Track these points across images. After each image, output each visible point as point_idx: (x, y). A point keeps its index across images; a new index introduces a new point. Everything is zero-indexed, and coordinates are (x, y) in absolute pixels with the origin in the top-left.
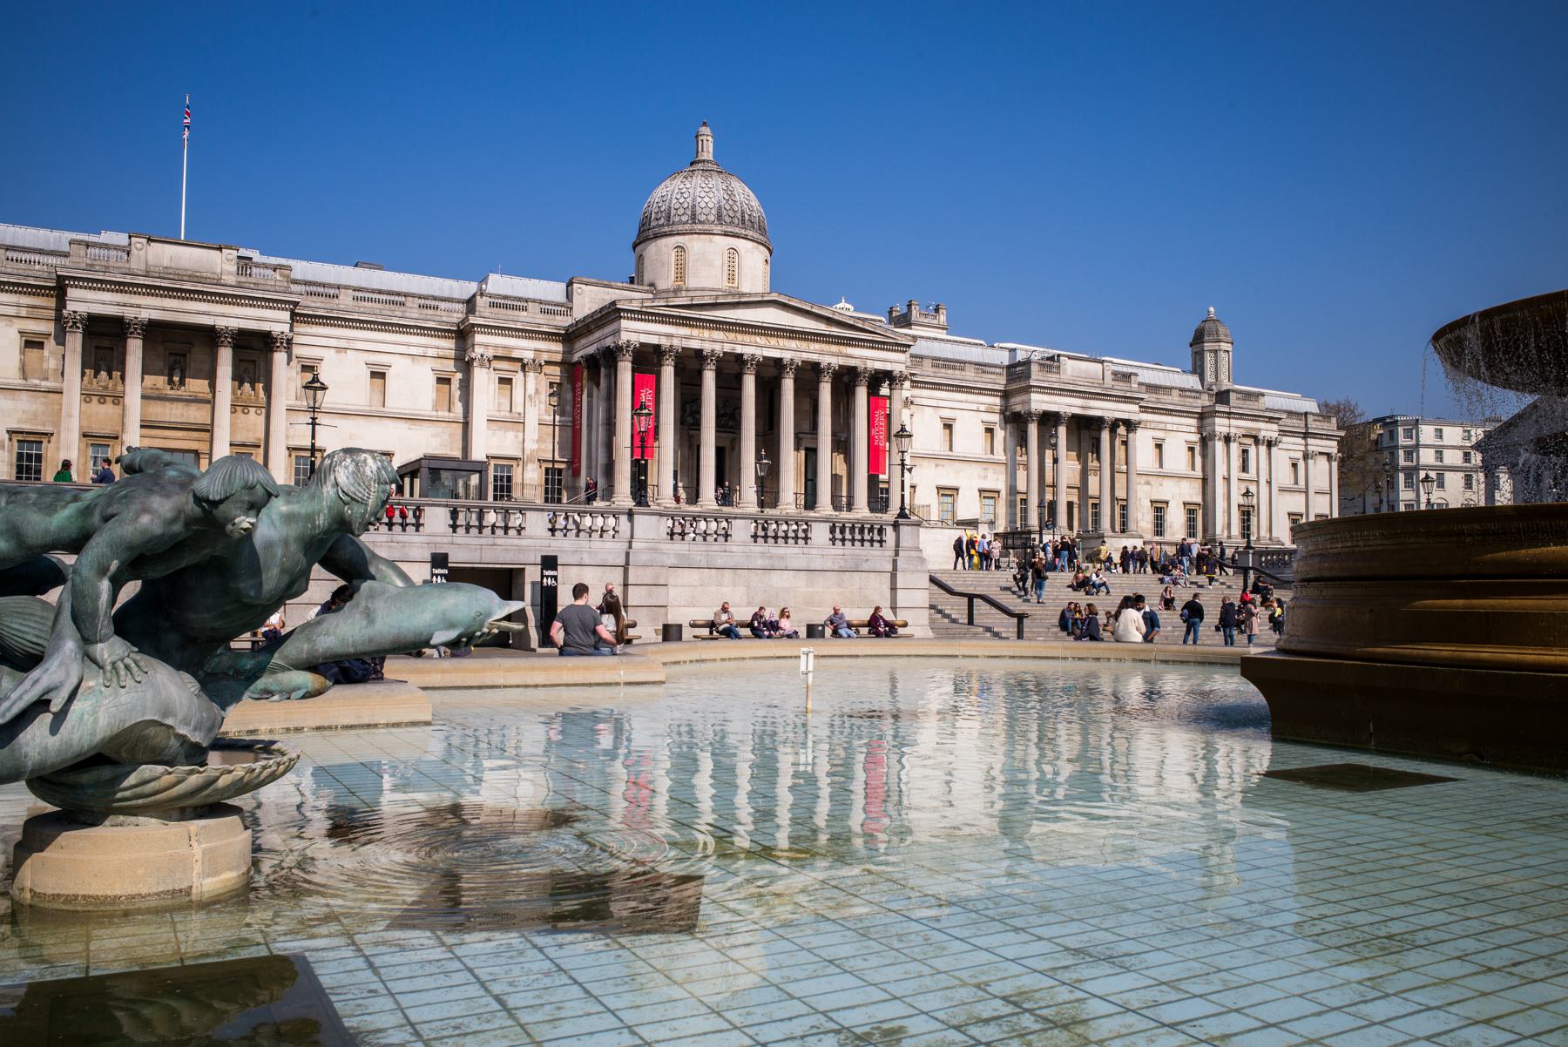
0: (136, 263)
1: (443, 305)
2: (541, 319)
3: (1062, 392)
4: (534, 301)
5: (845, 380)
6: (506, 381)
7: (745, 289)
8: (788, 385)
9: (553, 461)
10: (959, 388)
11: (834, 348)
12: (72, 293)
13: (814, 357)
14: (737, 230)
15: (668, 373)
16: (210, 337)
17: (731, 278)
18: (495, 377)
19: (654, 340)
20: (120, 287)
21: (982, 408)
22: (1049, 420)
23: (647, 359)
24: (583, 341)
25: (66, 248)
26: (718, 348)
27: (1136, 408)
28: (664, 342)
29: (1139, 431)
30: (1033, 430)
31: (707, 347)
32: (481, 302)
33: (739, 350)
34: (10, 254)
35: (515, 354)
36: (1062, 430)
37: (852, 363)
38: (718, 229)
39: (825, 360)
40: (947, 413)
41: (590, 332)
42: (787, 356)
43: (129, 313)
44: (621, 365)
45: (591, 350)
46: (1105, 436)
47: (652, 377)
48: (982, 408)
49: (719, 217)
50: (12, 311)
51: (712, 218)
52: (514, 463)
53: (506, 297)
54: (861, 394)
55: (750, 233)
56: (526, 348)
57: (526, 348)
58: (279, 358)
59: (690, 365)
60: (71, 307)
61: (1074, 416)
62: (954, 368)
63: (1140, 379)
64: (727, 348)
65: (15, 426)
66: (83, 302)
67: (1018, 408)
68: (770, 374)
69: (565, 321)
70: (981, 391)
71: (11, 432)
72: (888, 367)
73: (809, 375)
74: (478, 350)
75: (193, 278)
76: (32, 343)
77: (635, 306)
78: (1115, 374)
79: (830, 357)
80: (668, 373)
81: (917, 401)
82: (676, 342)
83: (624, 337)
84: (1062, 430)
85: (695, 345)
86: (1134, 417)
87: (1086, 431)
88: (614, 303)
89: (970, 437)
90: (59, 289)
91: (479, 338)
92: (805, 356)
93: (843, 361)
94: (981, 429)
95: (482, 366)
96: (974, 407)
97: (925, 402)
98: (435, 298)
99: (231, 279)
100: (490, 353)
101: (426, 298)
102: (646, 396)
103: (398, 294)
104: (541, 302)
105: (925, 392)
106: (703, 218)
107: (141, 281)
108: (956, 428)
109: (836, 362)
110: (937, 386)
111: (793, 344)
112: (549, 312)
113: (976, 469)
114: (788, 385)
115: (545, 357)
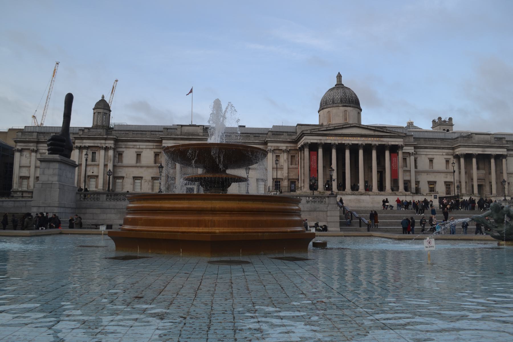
0: (178, 132)
1: (261, 135)
2: (287, 137)
3: (473, 146)
4: (285, 132)
5: (381, 149)
6: (277, 156)
7: (351, 122)
8: (361, 152)
9: (277, 179)
10: (435, 148)
11: (378, 139)
12: (164, 141)
13: (370, 142)
14: (347, 105)
15: (320, 151)
17: (346, 119)
18: (275, 155)
19: (315, 141)
20: (174, 139)
21: (444, 154)
22: (468, 157)
23: (313, 147)
24: (299, 143)
25: (162, 130)
26: (337, 142)
27: (505, 150)
28: (319, 142)
29: (508, 158)
30: (462, 160)
31: (333, 142)
32: (269, 133)
33: (343, 142)
34: (152, 133)
35: (280, 148)
36: (474, 160)
37: (383, 143)
38: (340, 105)
39: (374, 143)
40: (431, 157)
41: (300, 140)
42: (360, 143)
44: (305, 149)
45: (300, 146)
46: (493, 161)
47: (316, 152)
48: (444, 154)
49: (341, 101)
50: (152, 147)
51: (339, 102)
52: (281, 180)
53: (277, 132)
54: (387, 153)
55: (352, 105)
56: (283, 146)
57: (283, 146)
59: (327, 148)
60: (163, 145)
61: (479, 154)
62: (433, 141)
63: (506, 139)
64: (340, 142)
65: (153, 176)
66: (167, 143)
67: (457, 153)
68: (354, 149)
69: (294, 137)
70: (443, 148)
71: (152, 178)
72: (397, 143)
73: (368, 149)
74: (269, 148)
75: (193, 134)
76: (157, 155)
77: (309, 132)
78: (495, 138)
80: (320, 151)
81: (418, 153)
82: (323, 142)
83: (306, 141)
84: (474, 160)
85: (329, 142)
86: (505, 153)
87: (484, 159)
88: (302, 131)
89: (440, 163)
90: (161, 142)
91: (269, 144)
92: (366, 142)
93: (380, 143)
94: (444, 161)
95: (270, 152)
97: (422, 153)
98: (258, 134)
99: (202, 134)
100: (273, 149)
101: (256, 134)
102: (315, 157)
103: (248, 133)
104: (287, 132)
105: (422, 150)
106: (336, 102)
107: (179, 137)
108: (434, 161)
109: (377, 143)
110: (426, 148)
111: (363, 139)
112: (290, 135)
113: (443, 175)
114: (361, 152)
115: (289, 148)
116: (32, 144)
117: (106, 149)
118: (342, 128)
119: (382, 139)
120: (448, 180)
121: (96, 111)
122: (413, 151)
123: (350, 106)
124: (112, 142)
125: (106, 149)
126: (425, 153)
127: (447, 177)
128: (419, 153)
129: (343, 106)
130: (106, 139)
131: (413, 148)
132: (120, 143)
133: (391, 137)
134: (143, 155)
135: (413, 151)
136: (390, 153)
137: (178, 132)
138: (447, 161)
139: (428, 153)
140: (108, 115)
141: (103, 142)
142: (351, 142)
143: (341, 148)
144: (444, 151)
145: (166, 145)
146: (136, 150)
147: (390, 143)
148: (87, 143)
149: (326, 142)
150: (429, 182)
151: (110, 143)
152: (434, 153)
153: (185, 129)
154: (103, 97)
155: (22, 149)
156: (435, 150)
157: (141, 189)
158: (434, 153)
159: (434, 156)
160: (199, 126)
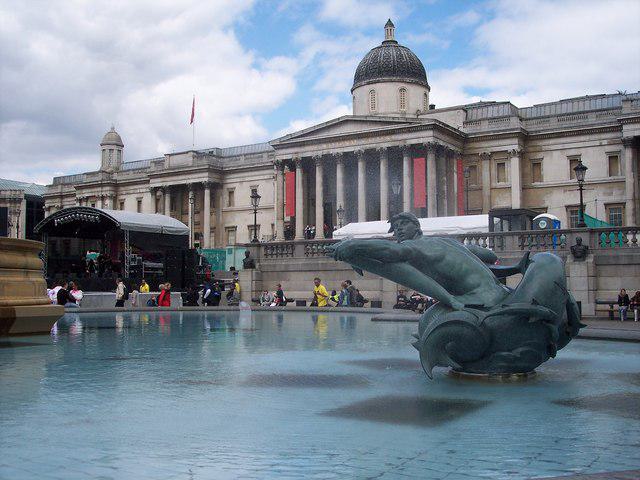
11: (388, 138)
15: (299, 172)
16: (183, 188)
19: (289, 157)
20: (161, 176)
26: (320, 153)
37: (397, 144)
42: (357, 149)
43: (164, 184)
48: (605, 142)
58: (207, 192)
59: (308, 165)
72: (421, 141)
79: (384, 143)
80: (299, 172)
82: (300, 156)
85: (308, 155)
94: (605, 159)
96: (598, 143)
99: (190, 164)
105: (552, 141)
109: (385, 146)
111: (363, 141)
116: (57, 200)
117: (103, 198)
118: (329, 127)
119: (394, 137)
120: (614, 199)
121: (105, 147)
122: (516, 147)
123: (379, 82)
124: (108, 188)
125: (103, 198)
126: (560, 147)
127: (611, 194)
128: (544, 148)
129: (368, 84)
130: (102, 185)
131: (516, 141)
132: (122, 189)
133: (409, 130)
134: (144, 201)
135: (516, 147)
136: (389, 167)
137: (166, 166)
138: (613, 158)
139: (566, 146)
140: (115, 152)
141: (99, 189)
142: (340, 151)
143: (328, 161)
144: (603, 136)
145: (153, 186)
146: (136, 196)
147: (409, 142)
148: (86, 193)
149: (305, 155)
150: (567, 207)
151: (107, 191)
152: (581, 145)
153: (176, 161)
154: (113, 129)
155: (50, 207)
156: (582, 138)
157: (215, 245)
158: (581, 145)
159: (582, 151)
160: (187, 152)
